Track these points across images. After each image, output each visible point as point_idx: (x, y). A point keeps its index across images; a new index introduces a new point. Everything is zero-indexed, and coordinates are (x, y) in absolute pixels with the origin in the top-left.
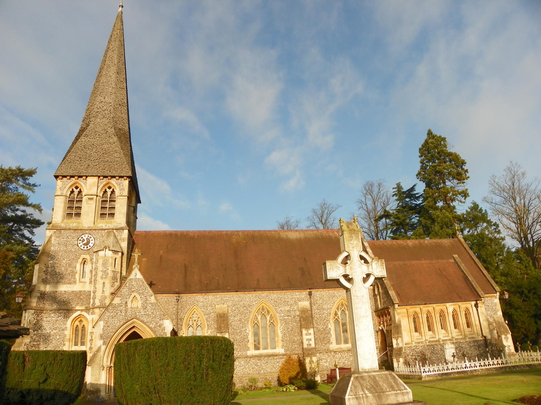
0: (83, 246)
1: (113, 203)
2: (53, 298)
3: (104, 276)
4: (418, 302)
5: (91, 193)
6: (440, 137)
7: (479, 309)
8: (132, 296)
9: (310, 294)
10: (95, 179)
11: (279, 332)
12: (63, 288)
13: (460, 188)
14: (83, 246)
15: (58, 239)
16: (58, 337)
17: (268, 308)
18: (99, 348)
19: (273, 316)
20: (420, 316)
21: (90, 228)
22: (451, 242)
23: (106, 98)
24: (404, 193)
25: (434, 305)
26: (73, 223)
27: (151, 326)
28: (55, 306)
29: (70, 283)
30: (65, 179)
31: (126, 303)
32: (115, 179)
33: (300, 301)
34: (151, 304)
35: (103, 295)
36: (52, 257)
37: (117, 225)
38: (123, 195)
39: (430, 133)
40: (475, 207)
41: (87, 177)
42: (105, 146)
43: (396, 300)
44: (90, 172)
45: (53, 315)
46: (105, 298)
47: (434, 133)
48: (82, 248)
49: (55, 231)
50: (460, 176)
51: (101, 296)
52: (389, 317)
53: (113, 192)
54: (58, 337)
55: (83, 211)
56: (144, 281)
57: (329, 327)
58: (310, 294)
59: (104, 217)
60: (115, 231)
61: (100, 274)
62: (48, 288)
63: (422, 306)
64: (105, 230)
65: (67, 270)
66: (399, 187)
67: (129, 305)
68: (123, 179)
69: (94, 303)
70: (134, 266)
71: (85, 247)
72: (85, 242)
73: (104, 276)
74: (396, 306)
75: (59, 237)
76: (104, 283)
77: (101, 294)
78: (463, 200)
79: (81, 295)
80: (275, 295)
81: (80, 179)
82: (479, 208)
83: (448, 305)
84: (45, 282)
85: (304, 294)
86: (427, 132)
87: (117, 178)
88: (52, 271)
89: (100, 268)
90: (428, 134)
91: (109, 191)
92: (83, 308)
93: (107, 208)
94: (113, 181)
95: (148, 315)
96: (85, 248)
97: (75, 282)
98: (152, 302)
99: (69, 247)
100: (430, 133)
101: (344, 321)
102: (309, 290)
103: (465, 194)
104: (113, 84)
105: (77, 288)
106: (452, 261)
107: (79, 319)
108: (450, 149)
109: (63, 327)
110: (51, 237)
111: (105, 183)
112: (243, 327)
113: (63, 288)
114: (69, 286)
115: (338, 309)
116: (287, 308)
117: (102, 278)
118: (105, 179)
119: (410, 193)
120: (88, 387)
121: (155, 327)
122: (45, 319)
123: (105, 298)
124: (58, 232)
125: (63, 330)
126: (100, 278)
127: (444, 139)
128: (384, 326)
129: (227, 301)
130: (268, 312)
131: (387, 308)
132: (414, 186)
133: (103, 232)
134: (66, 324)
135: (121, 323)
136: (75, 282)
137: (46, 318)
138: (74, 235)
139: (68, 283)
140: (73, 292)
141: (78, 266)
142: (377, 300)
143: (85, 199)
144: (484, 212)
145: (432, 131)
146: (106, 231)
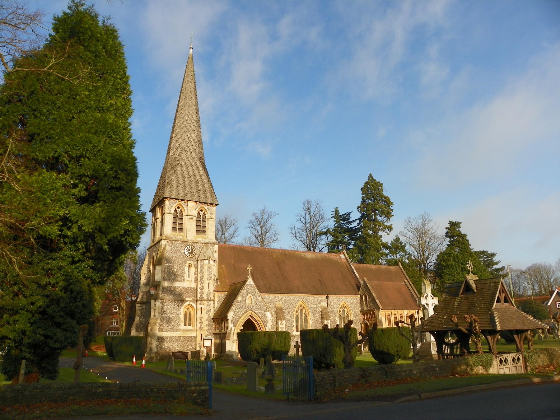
0: (188, 254)
1: (204, 223)
2: (170, 291)
3: (209, 278)
4: (391, 308)
5: (191, 214)
6: (379, 182)
7: (419, 314)
8: (248, 296)
9: (327, 298)
10: (194, 203)
11: (310, 320)
12: (177, 284)
13: (388, 224)
14: (188, 254)
15: (170, 247)
16: (175, 319)
17: (304, 305)
18: (231, 328)
19: (307, 310)
20: (391, 316)
21: (193, 241)
22: (396, 269)
23: (192, 135)
24: (341, 216)
25: (398, 311)
26: (178, 236)
27: (259, 315)
28: (172, 298)
29: (181, 281)
30: (171, 200)
31: (245, 300)
32: (206, 205)
33: (322, 302)
34: (259, 301)
35: (209, 291)
36: (168, 261)
37: (210, 240)
38: (213, 218)
39: (370, 177)
40: (397, 240)
41: (187, 201)
42: (198, 177)
43: (381, 307)
44: (190, 197)
45: (171, 304)
46: (210, 293)
47: (374, 178)
48: (188, 255)
49: (168, 241)
50: (388, 214)
51: (208, 292)
52: (373, 316)
53: (204, 214)
54: (175, 319)
55: (184, 227)
56: (255, 286)
57: (337, 319)
58: (327, 298)
59: (198, 233)
60: (209, 245)
61: (206, 277)
62: (166, 284)
63: (392, 311)
64: (203, 243)
65: (178, 271)
66: (337, 211)
67: (247, 302)
68: (212, 206)
69: (202, 296)
70: (248, 276)
71: (190, 255)
72: (190, 251)
73: (209, 278)
74: (381, 309)
75: (171, 246)
76: (209, 283)
77: (208, 291)
78: (388, 232)
79: (188, 290)
80: (308, 297)
81: (182, 201)
82: (400, 241)
83: (405, 311)
84: (164, 279)
85: (324, 297)
86: (369, 175)
87: (214, 205)
88: (168, 271)
89: (206, 272)
90: (369, 177)
91: (202, 213)
92: (191, 299)
93: (200, 226)
94: (205, 206)
95: (258, 308)
96: (190, 256)
97: (184, 280)
98: (260, 300)
99: (179, 254)
100: (370, 177)
101: (344, 316)
102: (327, 296)
103: (390, 228)
104: (195, 123)
105: (186, 284)
106: (404, 283)
107: (187, 307)
108: (385, 193)
109: (178, 312)
110: (165, 245)
111: (199, 207)
112: (290, 317)
113: (177, 284)
114: (180, 283)
115: (341, 308)
116: (315, 306)
117: (208, 279)
118: (200, 204)
119: (346, 217)
120: (226, 353)
121: (262, 316)
122: (166, 306)
123: (210, 293)
124: (170, 242)
125: (178, 314)
126: (206, 279)
127: (382, 184)
128: (368, 321)
129: (281, 299)
130: (304, 308)
131: (373, 310)
132: (350, 213)
133: (201, 245)
134: (180, 310)
135: (243, 313)
136: (184, 280)
137: (166, 305)
138: (182, 245)
139: (180, 281)
140: (183, 287)
141: (186, 269)
142: (364, 304)
143: (185, 218)
144: (403, 244)
145: (373, 176)
146: (203, 244)
